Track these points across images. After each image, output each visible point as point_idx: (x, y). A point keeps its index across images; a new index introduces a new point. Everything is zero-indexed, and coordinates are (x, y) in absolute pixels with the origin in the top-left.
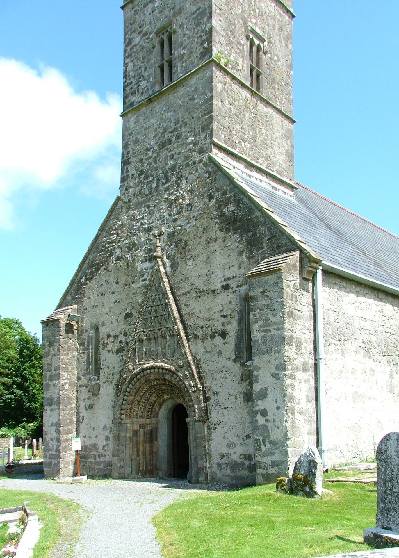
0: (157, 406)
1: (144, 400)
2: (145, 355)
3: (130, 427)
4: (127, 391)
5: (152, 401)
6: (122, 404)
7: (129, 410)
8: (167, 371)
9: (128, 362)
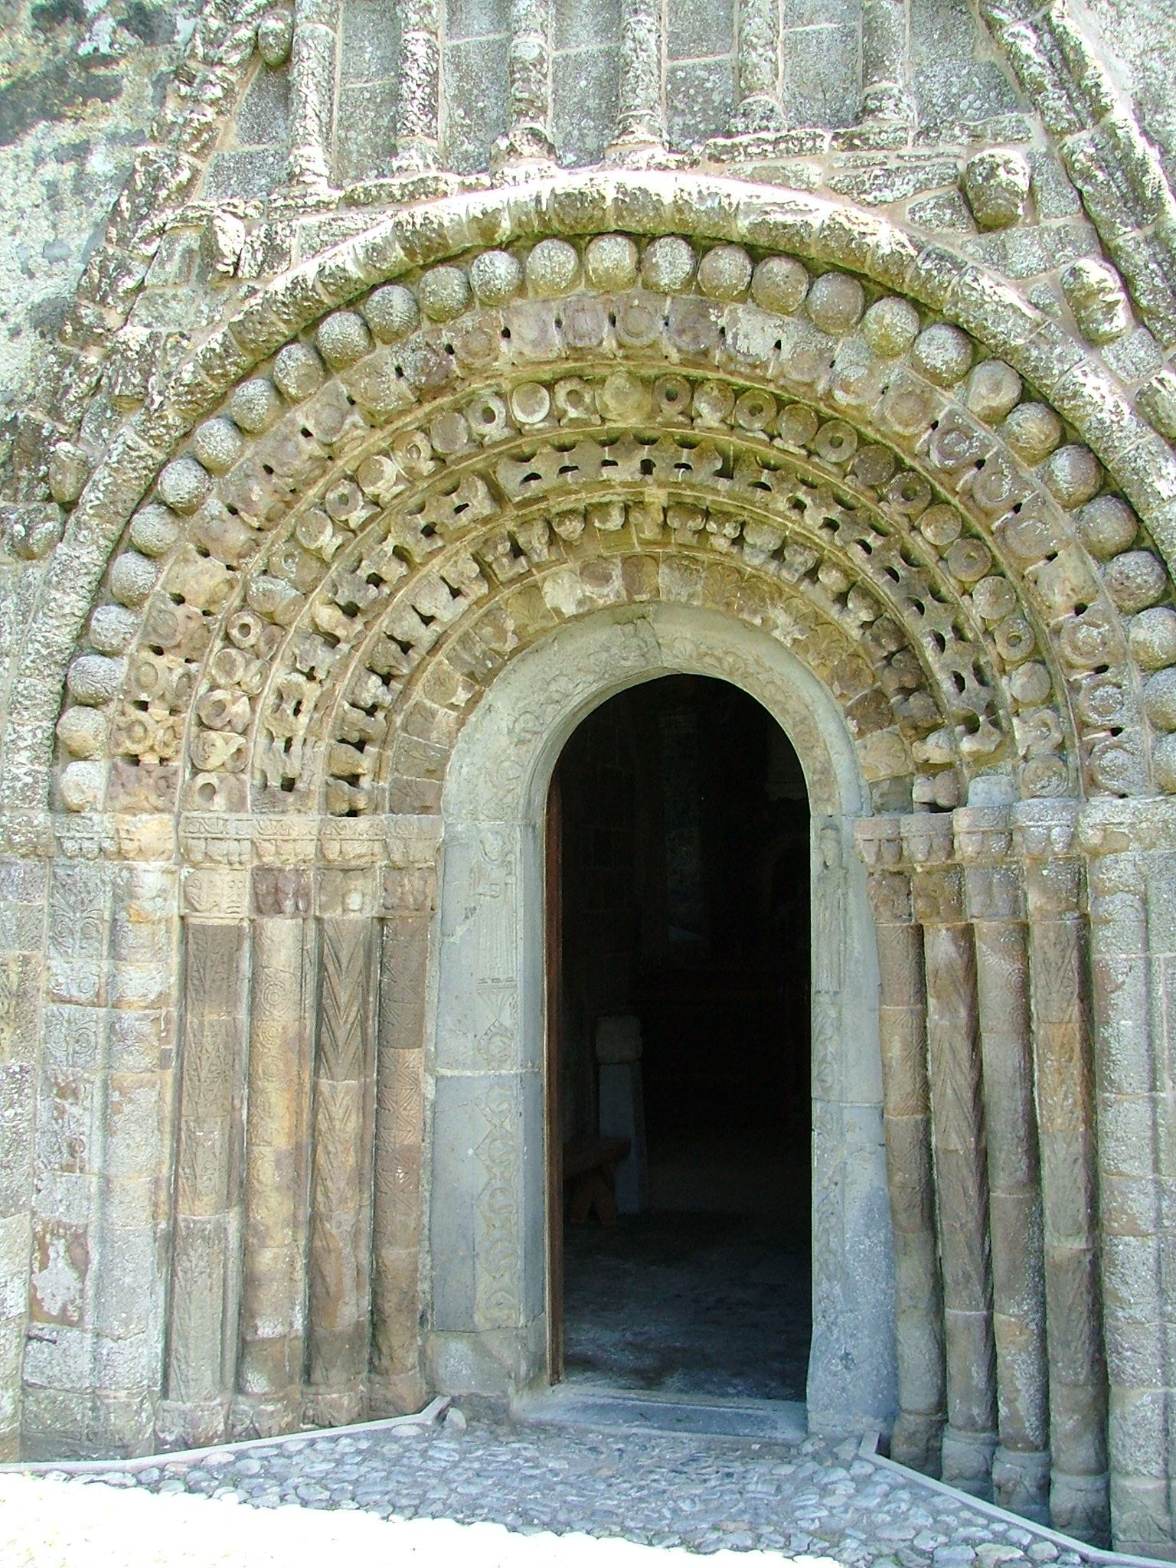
0: (441, 682)
1: (328, 617)
2: (431, 109)
3: (162, 893)
4: (149, 493)
5: (410, 627)
6: (84, 639)
7: (158, 711)
8: (779, 267)
9: (185, 190)
